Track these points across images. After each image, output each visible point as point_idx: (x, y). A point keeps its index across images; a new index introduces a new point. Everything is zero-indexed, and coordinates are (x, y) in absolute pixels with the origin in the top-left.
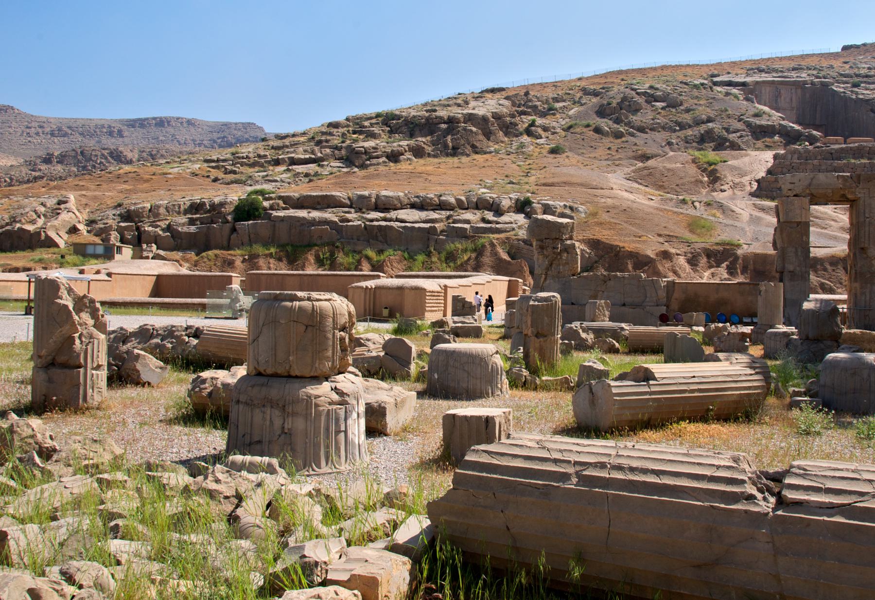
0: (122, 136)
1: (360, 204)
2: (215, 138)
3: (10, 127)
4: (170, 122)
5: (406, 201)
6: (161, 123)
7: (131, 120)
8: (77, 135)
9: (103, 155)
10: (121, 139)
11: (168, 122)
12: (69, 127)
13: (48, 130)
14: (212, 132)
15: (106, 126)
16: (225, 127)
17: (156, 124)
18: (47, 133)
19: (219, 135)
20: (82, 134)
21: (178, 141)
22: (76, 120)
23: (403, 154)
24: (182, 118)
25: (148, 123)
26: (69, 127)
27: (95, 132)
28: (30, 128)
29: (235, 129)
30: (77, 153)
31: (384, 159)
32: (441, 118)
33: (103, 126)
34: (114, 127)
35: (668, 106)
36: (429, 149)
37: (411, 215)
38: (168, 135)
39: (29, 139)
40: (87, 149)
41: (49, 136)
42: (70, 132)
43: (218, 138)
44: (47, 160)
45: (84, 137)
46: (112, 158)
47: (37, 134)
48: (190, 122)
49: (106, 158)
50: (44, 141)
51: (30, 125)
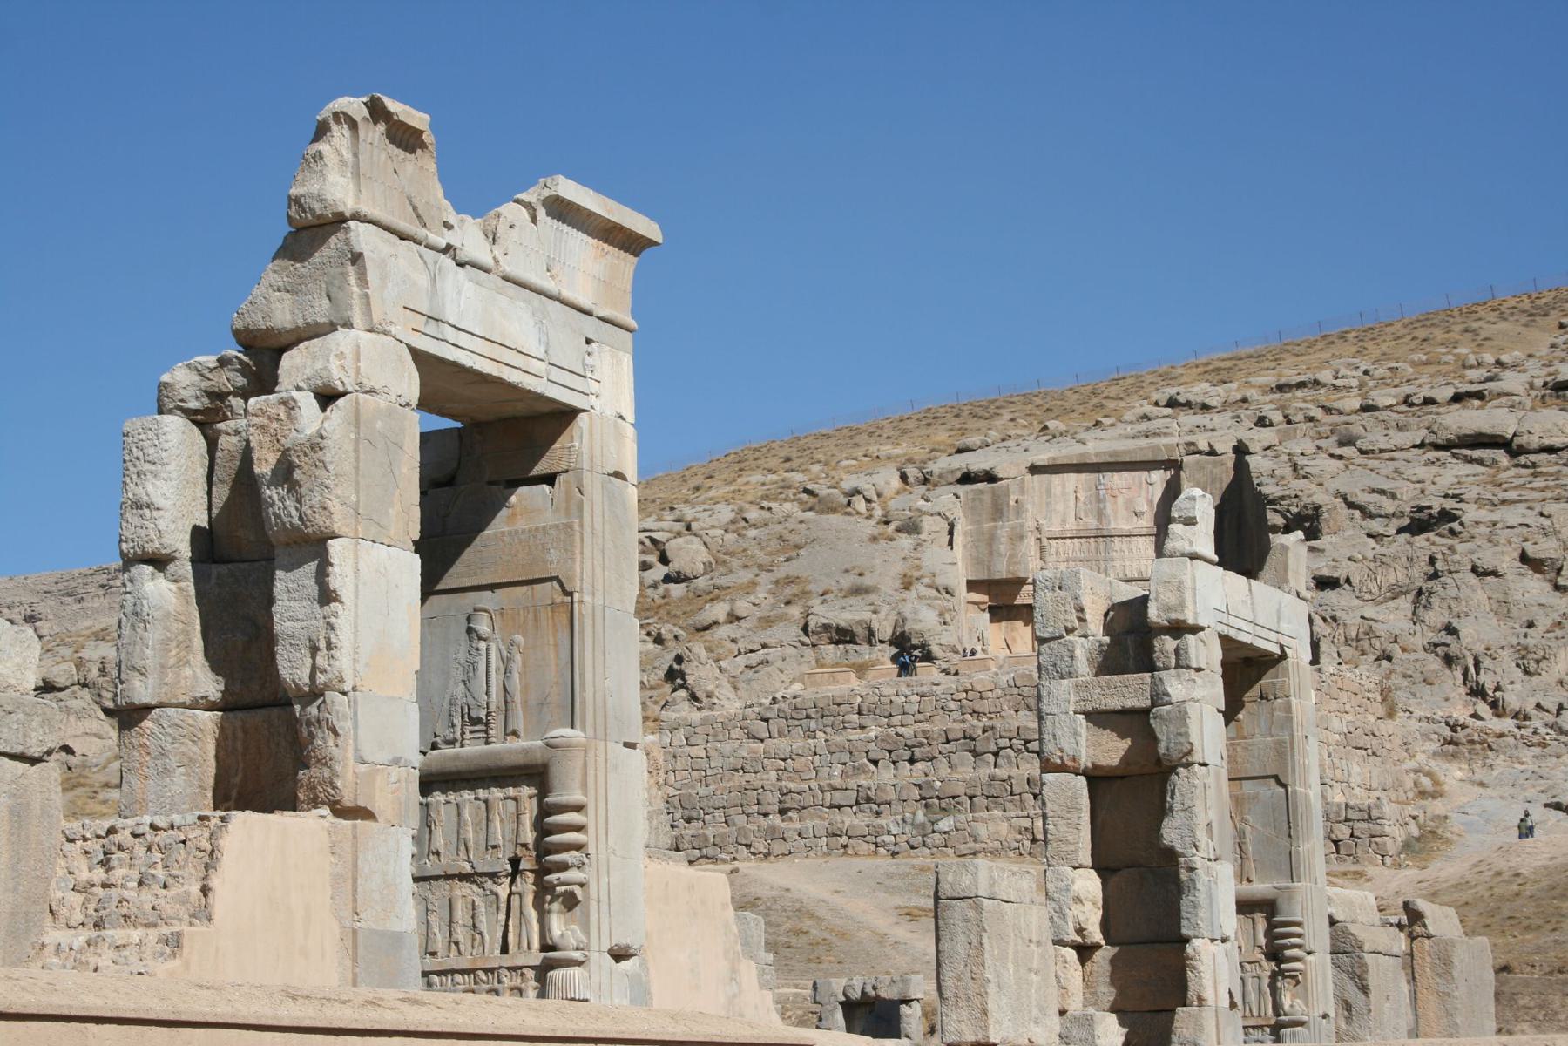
35: (668, 579)
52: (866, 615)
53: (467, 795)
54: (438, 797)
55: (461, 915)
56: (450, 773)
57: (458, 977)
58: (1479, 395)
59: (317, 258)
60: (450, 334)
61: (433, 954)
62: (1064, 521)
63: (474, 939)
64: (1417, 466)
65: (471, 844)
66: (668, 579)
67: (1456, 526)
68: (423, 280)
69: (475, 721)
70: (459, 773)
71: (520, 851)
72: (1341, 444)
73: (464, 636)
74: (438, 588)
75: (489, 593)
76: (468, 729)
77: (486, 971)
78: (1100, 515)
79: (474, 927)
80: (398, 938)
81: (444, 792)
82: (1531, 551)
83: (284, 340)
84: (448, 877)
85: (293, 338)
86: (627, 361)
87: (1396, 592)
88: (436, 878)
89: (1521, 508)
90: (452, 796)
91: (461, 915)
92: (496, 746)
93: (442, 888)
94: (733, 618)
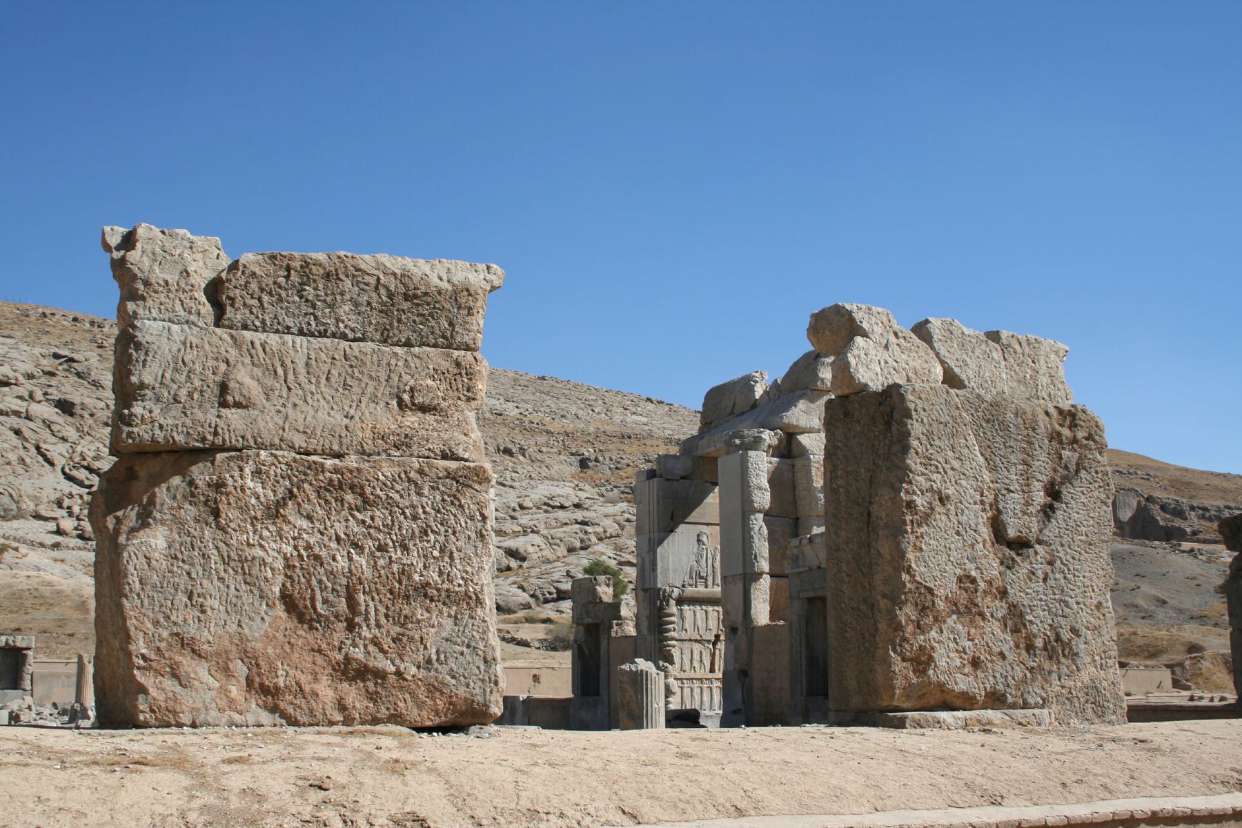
53: (698, 608)
54: (686, 607)
55: (696, 657)
56: (695, 598)
57: (694, 681)
59: (818, 403)
61: (684, 671)
63: (701, 666)
65: (700, 627)
69: (701, 578)
70: (698, 598)
71: (720, 632)
73: (696, 543)
74: (686, 521)
75: (705, 526)
76: (698, 580)
77: (706, 679)
79: (701, 661)
81: (689, 605)
83: (797, 431)
84: (690, 640)
85: (801, 430)
88: (685, 640)
90: (692, 607)
91: (696, 657)
92: (708, 589)
93: (687, 644)
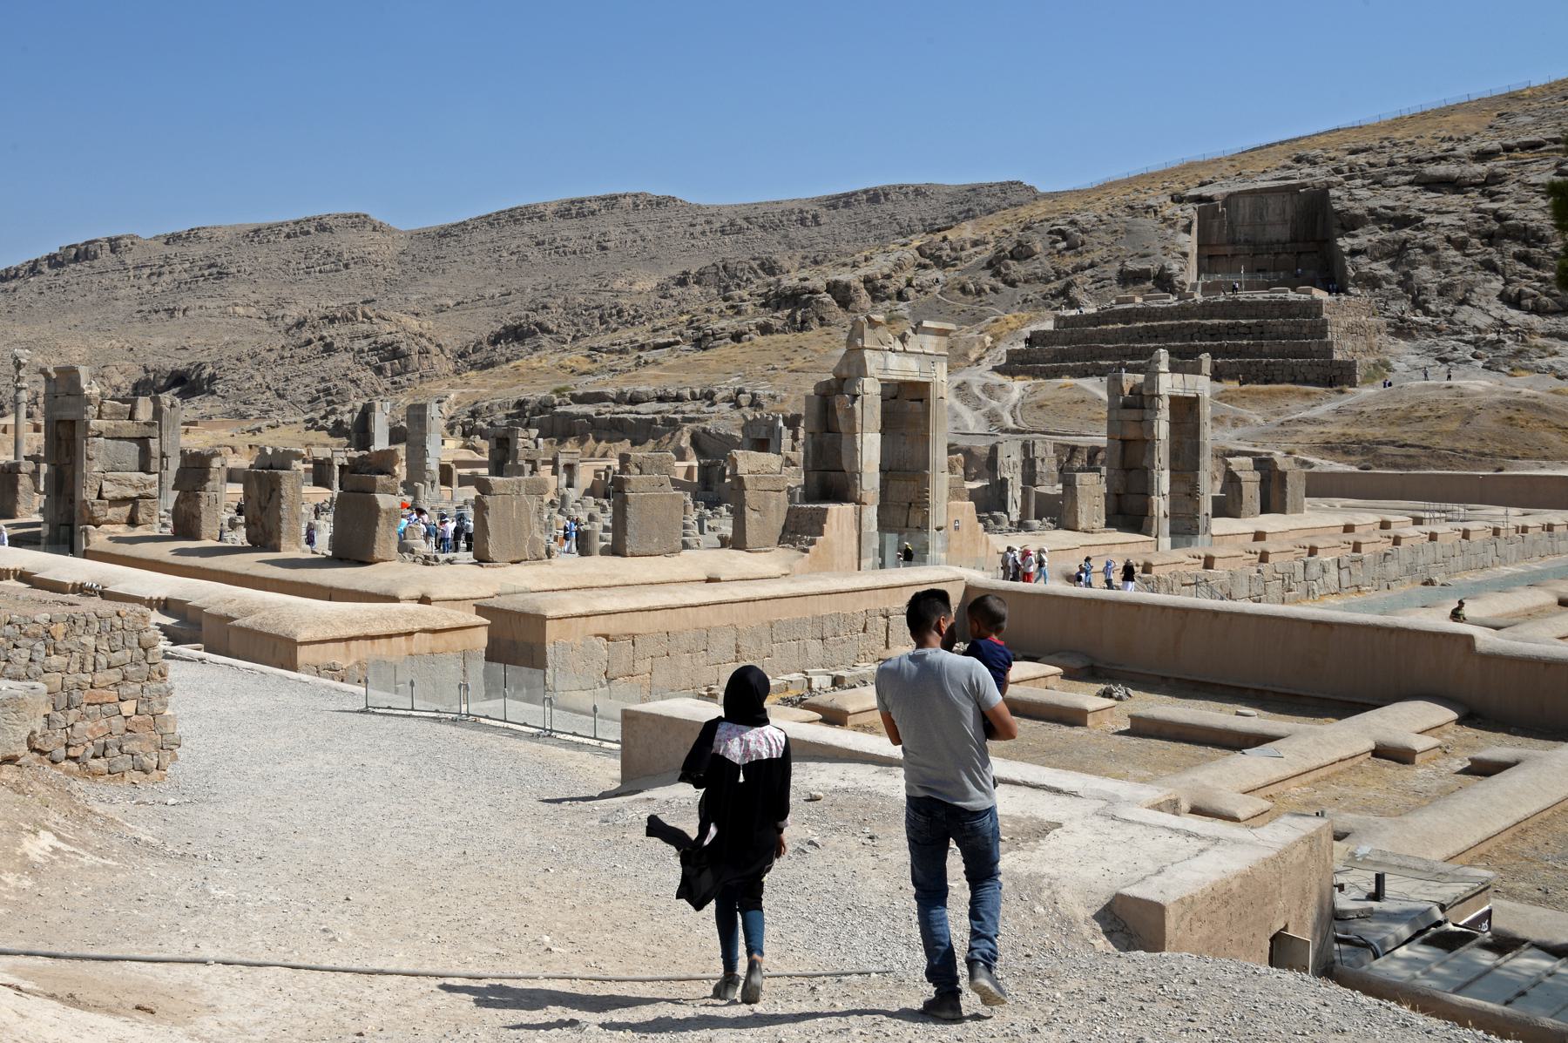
0: (818, 224)
1: (620, 399)
2: (955, 213)
3: (670, 227)
4: (888, 194)
5: (653, 395)
6: (874, 197)
7: (828, 198)
8: (757, 229)
9: (751, 268)
10: (817, 229)
11: (886, 195)
12: (747, 219)
13: (717, 225)
14: (951, 203)
15: (797, 211)
16: (973, 193)
17: (867, 200)
18: (716, 231)
19: (963, 207)
20: (762, 227)
21: (898, 223)
22: (756, 206)
23: (746, 334)
24: (908, 186)
25: (856, 200)
26: (747, 219)
27: (781, 222)
28: (695, 225)
29: (988, 196)
30: (718, 268)
31: (728, 340)
32: (805, 288)
33: (792, 212)
34: (807, 212)
36: (778, 324)
37: (655, 406)
38: (884, 216)
39: (692, 241)
40: (731, 261)
41: (719, 234)
42: (745, 225)
43: (960, 213)
44: (682, 282)
45: (766, 230)
46: (764, 270)
47: (703, 233)
48: (918, 192)
49: (755, 272)
50: (711, 242)
51: (694, 222)
52: (1148, 267)
58: (1444, 158)
60: (890, 372)
62: (1244, 218)
64: (1407, 193)
66: (1067, 249)
67: (1419, 224)
68: (882, 359)
72: (1374, 183)
78: (1261, 216)
80: (872, 533)
82: (1453, 237)
86: (945, 365)
87: (1387, 255)
89: (1452, 216)
94: (1092, 266)
